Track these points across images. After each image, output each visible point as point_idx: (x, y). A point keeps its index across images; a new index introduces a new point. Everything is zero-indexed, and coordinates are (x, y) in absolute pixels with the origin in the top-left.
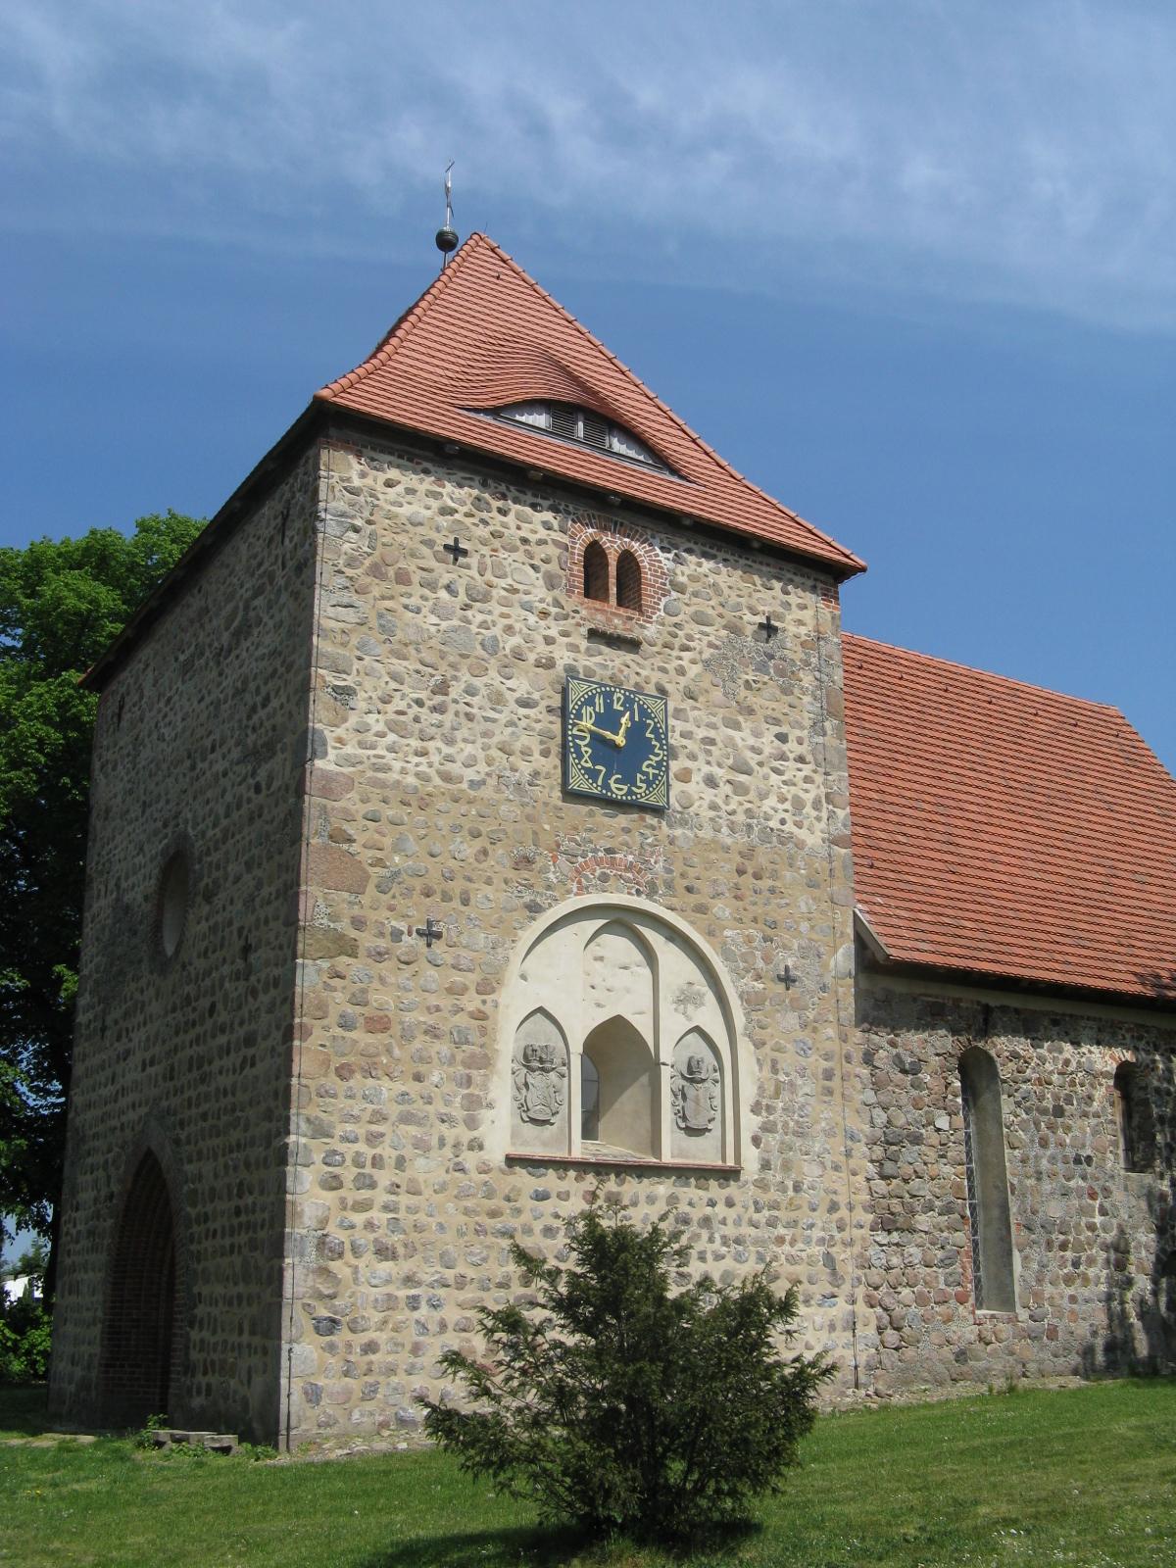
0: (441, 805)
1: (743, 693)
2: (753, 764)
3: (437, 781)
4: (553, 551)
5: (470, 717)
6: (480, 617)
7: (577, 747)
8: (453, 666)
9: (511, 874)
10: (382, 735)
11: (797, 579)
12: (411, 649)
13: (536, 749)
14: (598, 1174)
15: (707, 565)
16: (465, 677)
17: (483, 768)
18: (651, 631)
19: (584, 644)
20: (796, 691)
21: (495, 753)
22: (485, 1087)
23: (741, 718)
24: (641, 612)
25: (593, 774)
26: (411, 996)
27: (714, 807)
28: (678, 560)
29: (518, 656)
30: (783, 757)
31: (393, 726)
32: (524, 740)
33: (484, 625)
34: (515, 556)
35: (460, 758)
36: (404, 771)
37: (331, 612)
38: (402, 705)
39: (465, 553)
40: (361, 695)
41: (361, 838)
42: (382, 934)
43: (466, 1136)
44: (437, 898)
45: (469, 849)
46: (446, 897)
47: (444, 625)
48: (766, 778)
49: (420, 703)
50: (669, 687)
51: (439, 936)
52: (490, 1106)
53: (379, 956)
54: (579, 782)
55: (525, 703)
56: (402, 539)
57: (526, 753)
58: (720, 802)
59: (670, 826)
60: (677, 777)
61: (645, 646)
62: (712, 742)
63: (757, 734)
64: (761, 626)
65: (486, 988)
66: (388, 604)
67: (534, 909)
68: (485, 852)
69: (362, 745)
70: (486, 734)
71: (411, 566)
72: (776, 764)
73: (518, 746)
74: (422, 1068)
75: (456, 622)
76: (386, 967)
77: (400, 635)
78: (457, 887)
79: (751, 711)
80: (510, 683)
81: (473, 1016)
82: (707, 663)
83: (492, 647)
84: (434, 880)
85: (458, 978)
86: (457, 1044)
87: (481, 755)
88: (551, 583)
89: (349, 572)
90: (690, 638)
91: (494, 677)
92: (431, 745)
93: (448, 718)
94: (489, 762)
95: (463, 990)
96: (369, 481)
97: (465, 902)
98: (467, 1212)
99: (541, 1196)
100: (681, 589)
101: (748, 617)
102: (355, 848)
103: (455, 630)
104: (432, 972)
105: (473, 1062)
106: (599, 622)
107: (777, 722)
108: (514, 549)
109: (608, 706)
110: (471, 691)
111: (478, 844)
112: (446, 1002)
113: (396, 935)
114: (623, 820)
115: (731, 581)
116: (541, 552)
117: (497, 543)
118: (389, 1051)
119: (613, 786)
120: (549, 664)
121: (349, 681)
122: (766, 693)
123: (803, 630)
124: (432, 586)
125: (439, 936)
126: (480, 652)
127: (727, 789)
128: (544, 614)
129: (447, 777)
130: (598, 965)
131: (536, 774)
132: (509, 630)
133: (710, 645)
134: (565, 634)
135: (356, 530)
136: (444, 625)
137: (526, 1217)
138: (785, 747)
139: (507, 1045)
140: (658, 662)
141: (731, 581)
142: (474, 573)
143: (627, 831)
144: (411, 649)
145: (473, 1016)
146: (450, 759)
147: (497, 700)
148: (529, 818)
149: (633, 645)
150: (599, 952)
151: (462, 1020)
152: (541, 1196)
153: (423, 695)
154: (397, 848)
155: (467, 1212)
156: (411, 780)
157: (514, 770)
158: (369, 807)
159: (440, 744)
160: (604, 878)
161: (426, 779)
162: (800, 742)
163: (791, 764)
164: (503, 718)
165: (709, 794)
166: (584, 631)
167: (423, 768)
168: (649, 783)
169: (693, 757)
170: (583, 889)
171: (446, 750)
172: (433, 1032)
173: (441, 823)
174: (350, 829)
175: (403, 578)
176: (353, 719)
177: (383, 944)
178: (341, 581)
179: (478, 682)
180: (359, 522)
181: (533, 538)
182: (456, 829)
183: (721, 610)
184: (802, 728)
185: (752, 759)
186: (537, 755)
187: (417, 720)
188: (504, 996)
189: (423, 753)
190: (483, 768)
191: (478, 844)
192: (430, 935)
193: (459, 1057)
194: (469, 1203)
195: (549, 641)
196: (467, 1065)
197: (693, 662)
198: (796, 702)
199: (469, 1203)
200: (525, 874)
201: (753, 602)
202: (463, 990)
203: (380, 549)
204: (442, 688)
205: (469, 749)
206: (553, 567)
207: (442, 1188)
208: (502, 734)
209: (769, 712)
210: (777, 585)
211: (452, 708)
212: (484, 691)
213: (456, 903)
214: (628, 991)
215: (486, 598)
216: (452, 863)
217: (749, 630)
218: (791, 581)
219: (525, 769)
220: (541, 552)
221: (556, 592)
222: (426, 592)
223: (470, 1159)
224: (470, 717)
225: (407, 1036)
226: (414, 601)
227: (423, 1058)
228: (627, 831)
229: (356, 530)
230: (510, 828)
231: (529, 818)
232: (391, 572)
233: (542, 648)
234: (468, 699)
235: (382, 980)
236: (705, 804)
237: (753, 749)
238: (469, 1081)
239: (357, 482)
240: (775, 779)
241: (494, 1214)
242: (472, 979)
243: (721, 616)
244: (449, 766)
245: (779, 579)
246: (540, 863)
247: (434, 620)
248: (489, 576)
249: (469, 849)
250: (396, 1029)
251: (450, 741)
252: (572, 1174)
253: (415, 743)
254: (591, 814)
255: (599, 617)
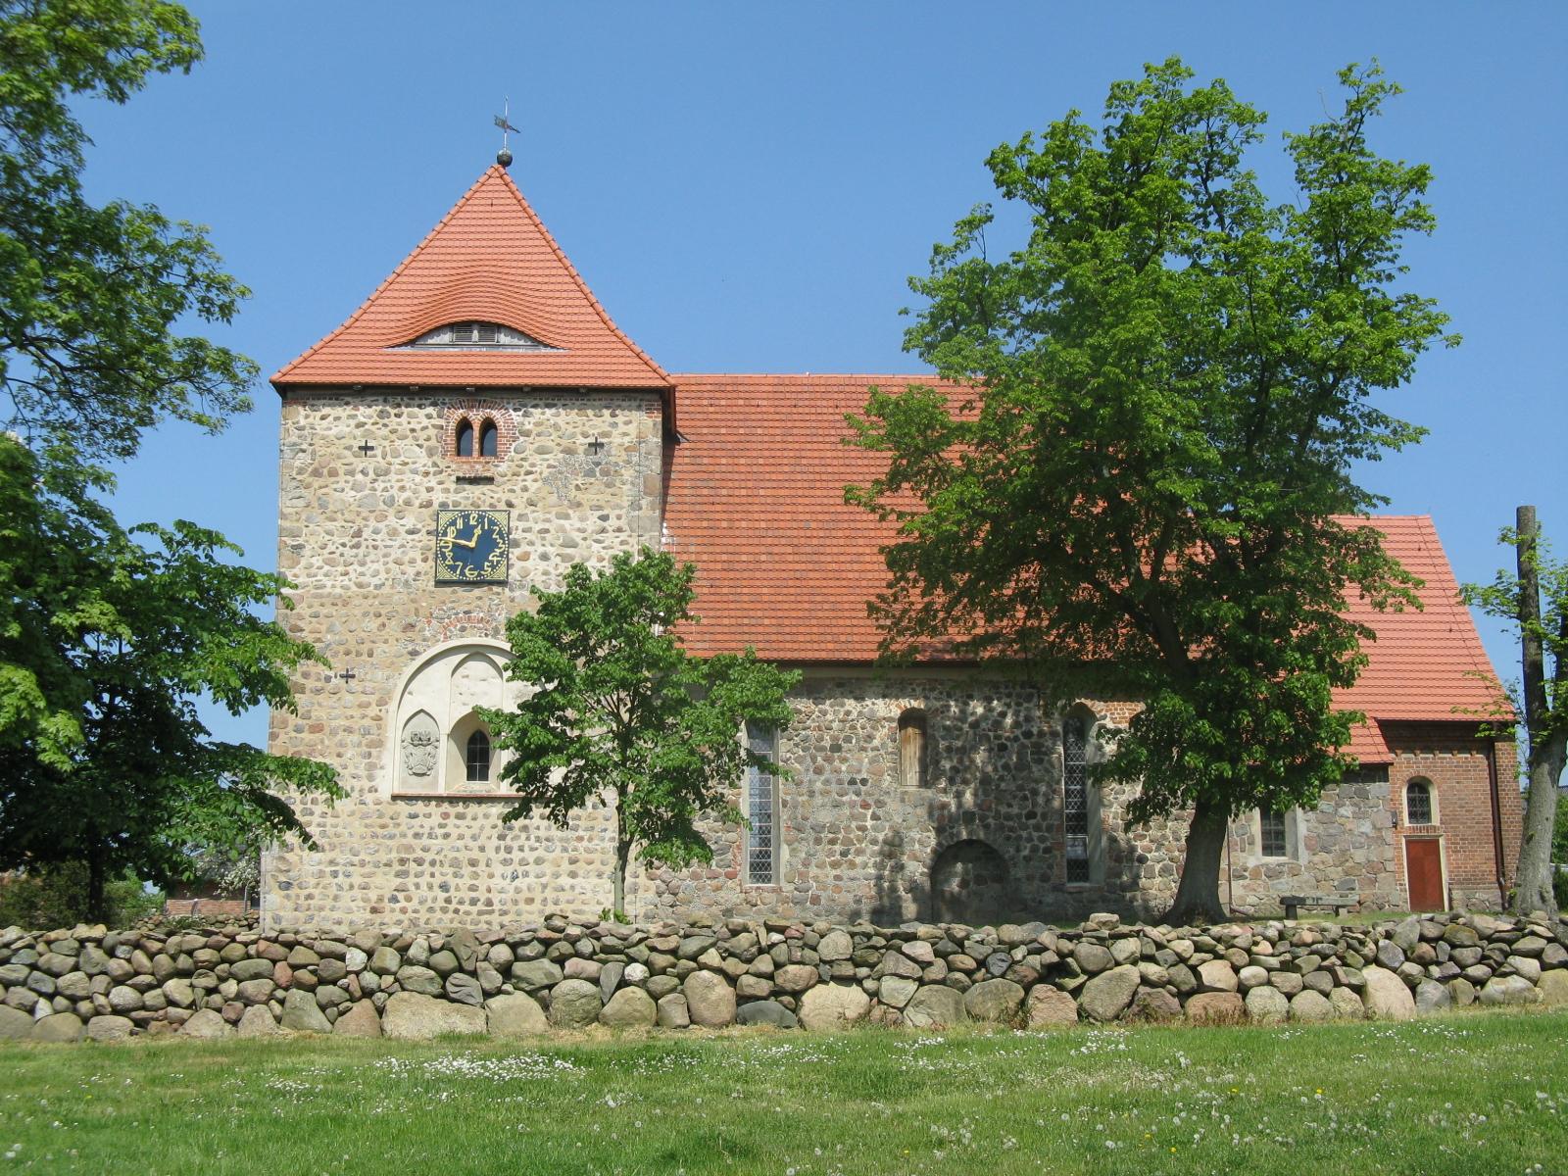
0: (357, 602)
1: (574, 492)
2: (579, 540)
3: (354, 588)
4: (432, 432)
5: (375, 547)
6: (383, 485)
7: (443, 554)
8: (364, 519)
9: (400, 635)
10: (320, 568)
11: (624, 404)
12: (339, 515)
13: (419, 558)
14: (451, 802)
15: (549, 412)
16: (372, 523)
17: (383, 576)
18: (503, 467)
19: (453, 486)
20: (618, 484)
21: (392, 565)
22: (379, 757)
23: (570, 512)
24: (496, 457)
25: (453, 568)
26: (337, 711)
27: (546, 573)
28: (526, 415)
29: (408, 503)
30: (603, 531)
31: (327, 562)
32: (411, 554)
33: (385, 490)
34: (405, 442)
35: (368, 573)
36: (333, 586)
37: (288, 503)
38: (333, 549)
39: (372, 448)
40: (308, 547)
41: (307, 628)
42: (319, 680)
43: (367, 784)
44: (353, 655)
45: (373, 624)
46: (359, 654)
47: (359, 495)
48: (589, 547)
49: (344, 545)
50: (514, 501)
51: (353, 676)
52: (382, 768)
53: (318, 691)
54: (447, 575)
55: (411, 532)
56: (333, 449)
57: (412, 562)
58: (551, 569)
59: (511, 590)
60: (519, 559)
61: (498, 479)
62: (547, 531)
63: (582, 520)
64: (590, 445)
65: (382, 703)
66: (324, 490)
67: (414, 654)
68: (384, 625)
69: (308, 576)
70: (385, 556)
71: (338, 465)
72: (598, 537)
73: (406, 559)
74: (342, 750)
75: (367, 492)
76: (320, 698)
77: (331, 507)
78: (365, 648)
79: (579, 505)
80: (402, 522)
81: (373, 719)
82: (545, 480)
83: (390, 502)
84: (352, 646)
85: (364, 698)
86: (363, 735)
87: (382, 568)
88: (431, 453)
89: (299, 477)
90: (533, 465)
91: (392, 520)
92: (350, 569)
93: (361, 551)
94: (388, 572)
95: (369, 704)
96: (310, 420)
97: (370, 655)
98: (366, 826)
99: (414, 816)
100: (527, 434)
101: (581, 440)
102: (304, 634)
103: (366, 497)
104: (349, 697)
105: (371, 745)
106: (466, 471)
107: (600, 508)
108: (406, 437)
109: (466, 524)
110: (376, 532)
111: (380, 621)
112: (357, 713)
113: (328, 679)
114: (477, 592)
115: (568, 419)
116: (423, 435)
117: (393, 437)
118: (322, 742)
119: (467, 571)
120: (429, 504)
121: (300, 541)
122: (593, 490)
123: (627, 439)
124: (352, 473)
125: (353, 676)
126: (383, 506)
127: (559, 559)
128: (427, 474)
129: (360, 586)
130: (465, 680)
131: (418, 574)
132: (402, 489)
133: (549, 466)
134: (441, 483)
135: (304, 451)
136: (359, 495)
137: (403, 828)
138: (606, 524)
139: (395, 733)
140: (509, 486)
141: (568, 419)
142: (379, 459)
143: (480, 598)
144: (339, 515)
145: (373, 719)
146: (362, 574)
147: (393, 533)
148: (413, 601)
149: (490, 480)
150: (466, 672)
151: (367, 722)
152: (414, 816)
153: (345, 540)
154: (329, 630)
155: (366, 826)
156: (338, 591)
157: (404, 573)
158: (313, 610)
159: (355, 566)
160: (463, 629)
161: (347, 588)
162: (619, 517)
163: (611, 534)
164: (397, 544)
165: (543, 566)
166: (454, 478)
167: (346, 582)
168: (493, 567)
169: (531, 543)
170: (446, 638)
171: (360, 569)
172: (349, 730)
173: (356, 612)
174: (301, 624)
175: (333, 473)
176: (303, 562)
177: (319, 685)
178: (295, 483)
179: (381, 525)
180: (304, 447)
181: (418, 427)
182: (366, 614)
183: (558, 440)
184: (622, 508)
185: (577, 537)
186: (419, 561)
187: (342, 555)
188: (393, 706)
189: (346, 574)
190: (383, 576)
191: (380, 621)
192: (348, 677)
193: (364, 742)
194: (368, 821)
195: (429, 490)
196: (367, 746)
197: (535, 481)
198: (617, 491)
199: (368, 821)
200: (410, 634)
201: (585, 429)
202: (369, 704)
203: (318, 459)
204: (358, 534)
205: (375, 566)
206: (433, 442)
207: (352, 814)
208: (396, 553)
209: (595, 503)
210: (606, 412)
211: (364, 544)
212: (385, 530)
213: (365, 657)
214: (486, 694)
215: (387, 473)
216: (363, 635)
217: (581, 450)
218: (619, 406)
219: (411, 571)
220: (423, 435)
221: (435, 458)
222: (349, 478)
223: (369, 798)
224: (375, 547)
225: (333, 732)
226: (341, 485)
227: (342, 745)
228: (480, 598)
229: (304, 451)
230: (400, 609)
231: (413, 601)
232: (325, 471)
233: (424, 496)
234: (375, 536)
235: (320, 705)
236: (539, 572)
237: (579, 530)
238: (370, 754)
239: (303, 422)
240: (596, 547)
241: (383, 827)
242: (373, 699)
243: (559, 445)
244: (362, 579)
245: (607, 408)
246: (419, 626)
247: (353, 493)
248: (389, 458)
249: (373, 624)
250: (327, 730)
251: (362, 564)
252: (434, 803)
253: (341, 569)
254: (454, 592)
255: (465, 467)
